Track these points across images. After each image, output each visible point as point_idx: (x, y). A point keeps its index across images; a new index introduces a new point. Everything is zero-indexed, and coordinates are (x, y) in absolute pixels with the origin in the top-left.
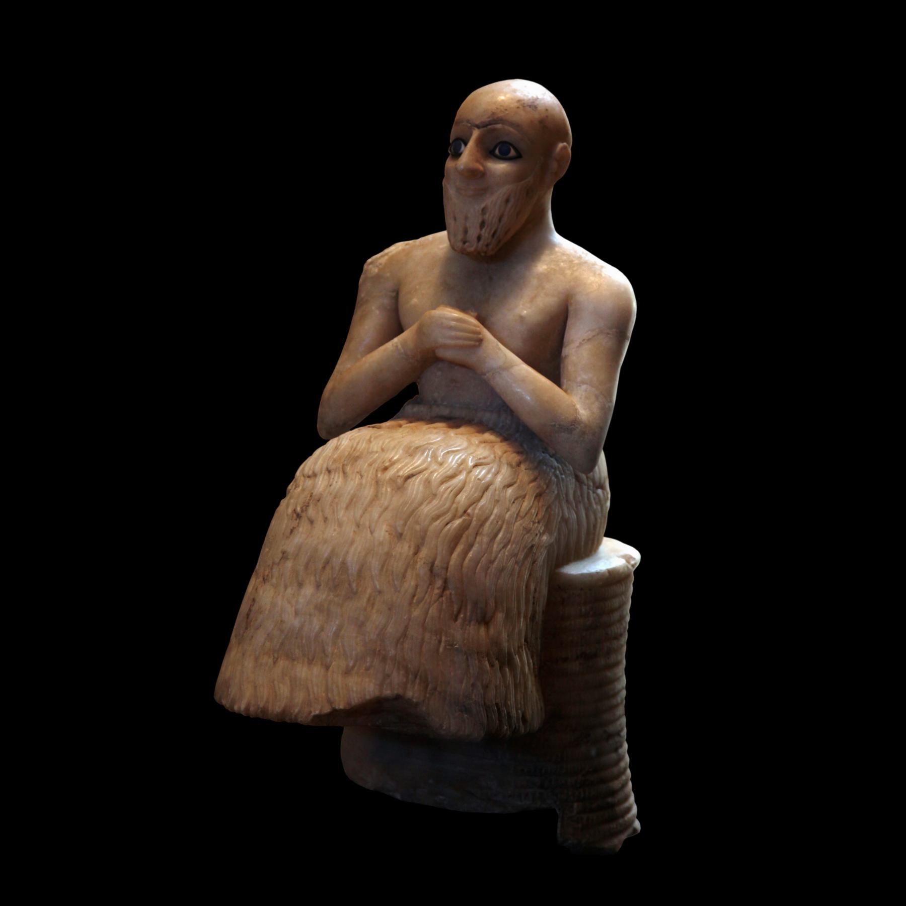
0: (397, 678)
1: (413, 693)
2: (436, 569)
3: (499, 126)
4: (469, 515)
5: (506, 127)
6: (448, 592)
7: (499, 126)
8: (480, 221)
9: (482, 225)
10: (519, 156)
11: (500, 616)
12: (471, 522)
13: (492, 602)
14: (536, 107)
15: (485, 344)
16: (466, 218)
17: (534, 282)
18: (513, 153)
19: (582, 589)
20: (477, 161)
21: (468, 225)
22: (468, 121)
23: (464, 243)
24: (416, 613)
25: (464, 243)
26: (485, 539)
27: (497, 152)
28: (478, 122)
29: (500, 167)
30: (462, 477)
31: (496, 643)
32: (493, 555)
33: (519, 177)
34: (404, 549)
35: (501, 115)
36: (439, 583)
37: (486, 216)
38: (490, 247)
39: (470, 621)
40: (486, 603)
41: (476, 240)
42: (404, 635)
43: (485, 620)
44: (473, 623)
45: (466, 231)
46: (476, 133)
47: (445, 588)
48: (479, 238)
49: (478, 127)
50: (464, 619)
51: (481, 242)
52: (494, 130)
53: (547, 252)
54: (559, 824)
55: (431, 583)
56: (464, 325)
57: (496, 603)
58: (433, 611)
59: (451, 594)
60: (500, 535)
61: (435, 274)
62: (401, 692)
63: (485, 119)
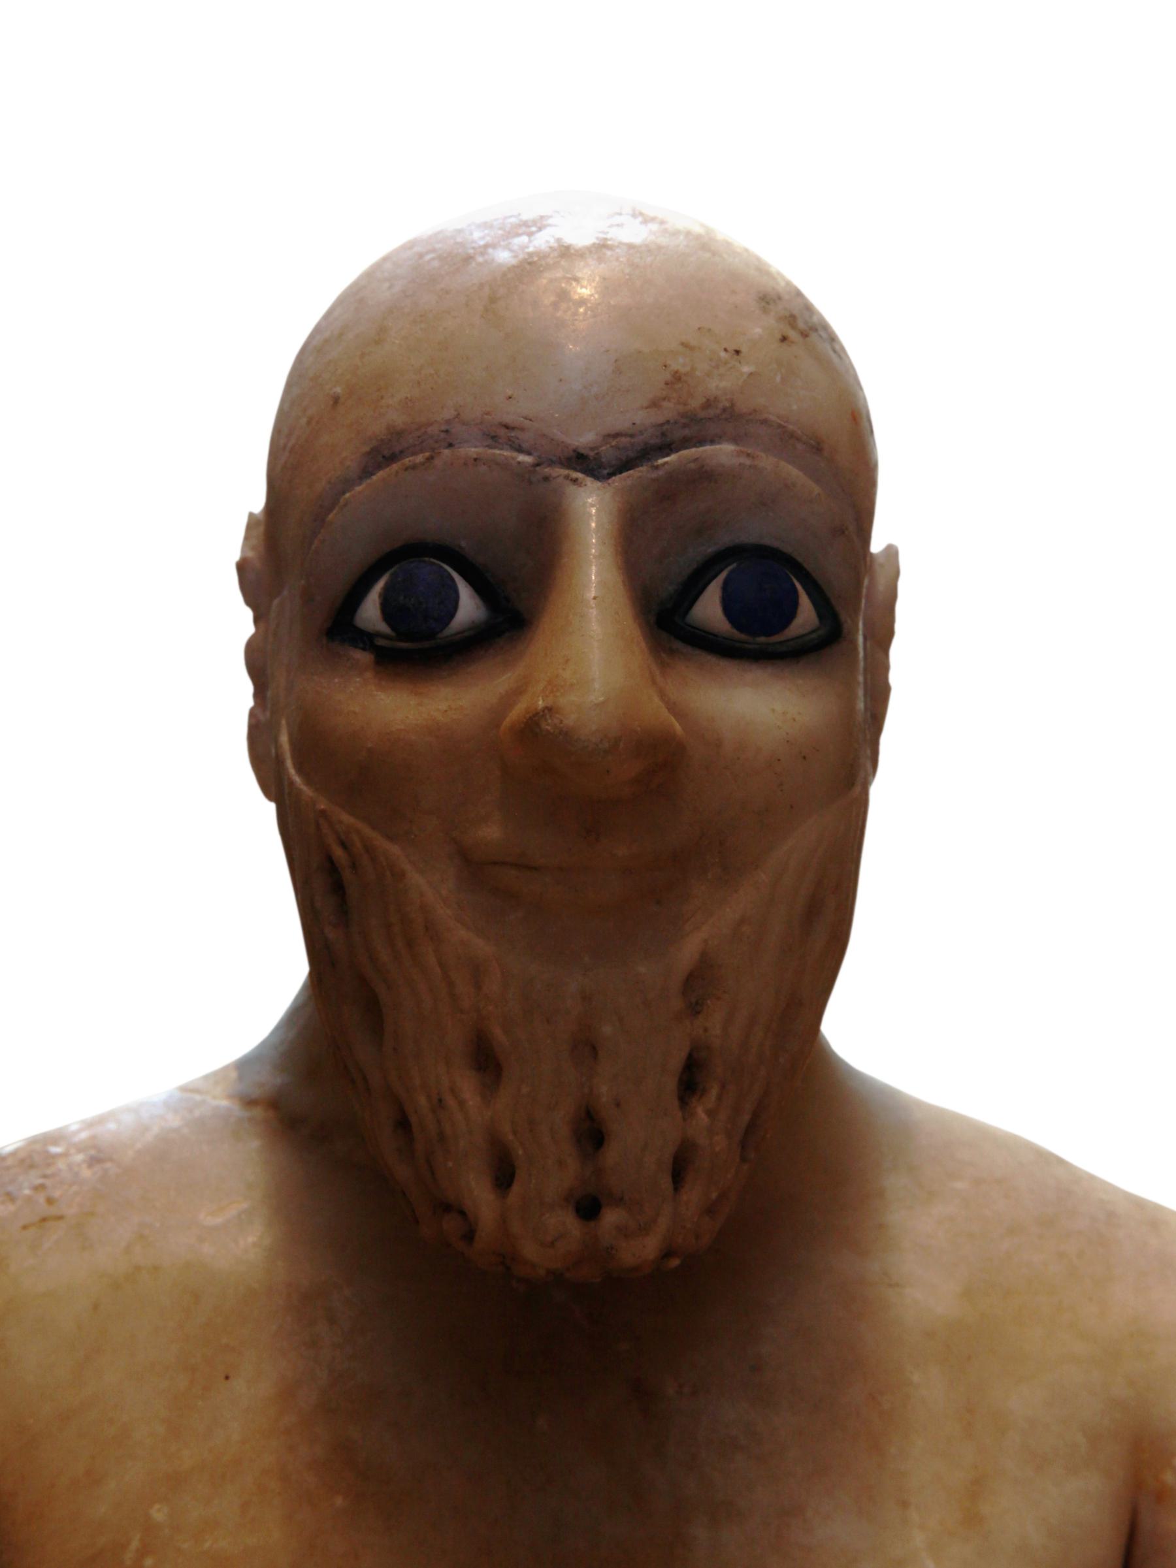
3: (723, 453)
5: (767, 462)
7: (722, 453)
8: (677, 1061)
9: (691, 1081)
16: (587, 1048)
17: (929, 1388)
21: (604, 1091)
22: (502, 434)
23: (588, 1208)
25: (588, 1208)
27: (709, 610)
28: (584, 439)
35: (719, 385)
37: (713, 1023)
41: (666, 1182)
45: (591, 1133)
46: (592, 510)
48: (680, 1168)
49: (586, 463)
51: (694, 1195)
52: (703, 476)
53: (895, 1183)
61: (248, 1404)
63: (632, 415)
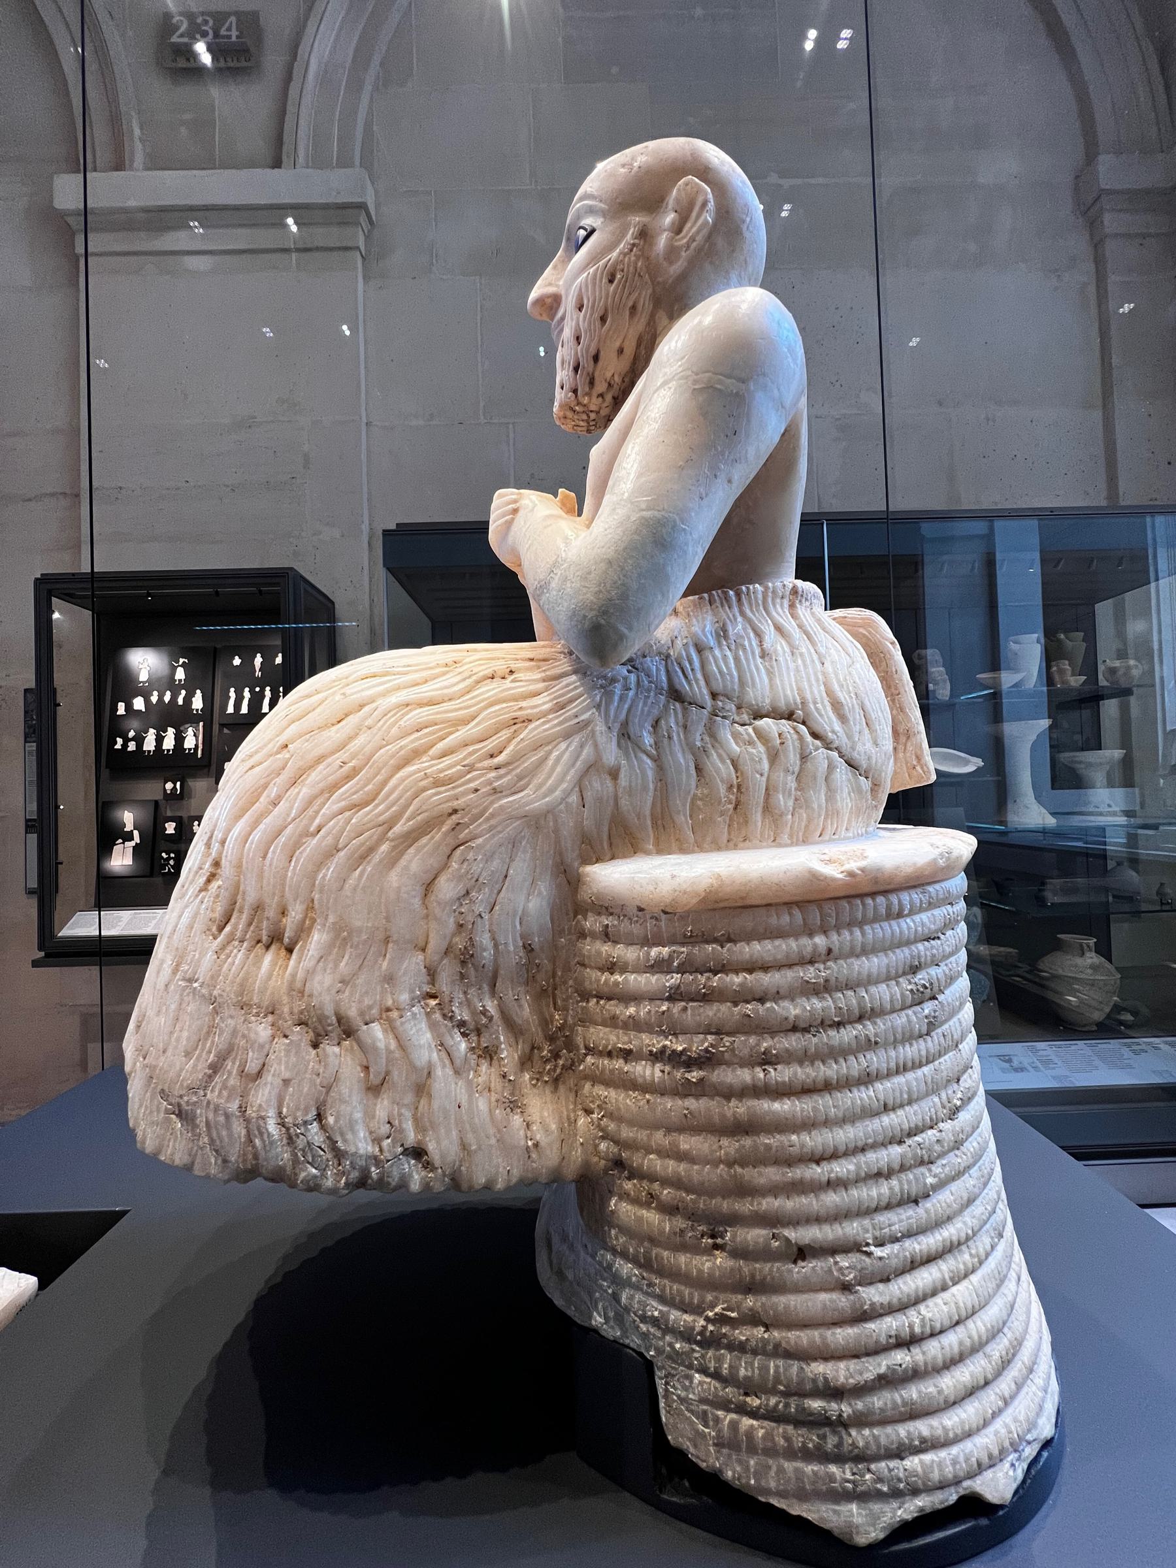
11: (317, 939)
13: (295, 913)
31: (299, 991)
43: (280, 941)
50: (230, 939)
54: (662, 1405)
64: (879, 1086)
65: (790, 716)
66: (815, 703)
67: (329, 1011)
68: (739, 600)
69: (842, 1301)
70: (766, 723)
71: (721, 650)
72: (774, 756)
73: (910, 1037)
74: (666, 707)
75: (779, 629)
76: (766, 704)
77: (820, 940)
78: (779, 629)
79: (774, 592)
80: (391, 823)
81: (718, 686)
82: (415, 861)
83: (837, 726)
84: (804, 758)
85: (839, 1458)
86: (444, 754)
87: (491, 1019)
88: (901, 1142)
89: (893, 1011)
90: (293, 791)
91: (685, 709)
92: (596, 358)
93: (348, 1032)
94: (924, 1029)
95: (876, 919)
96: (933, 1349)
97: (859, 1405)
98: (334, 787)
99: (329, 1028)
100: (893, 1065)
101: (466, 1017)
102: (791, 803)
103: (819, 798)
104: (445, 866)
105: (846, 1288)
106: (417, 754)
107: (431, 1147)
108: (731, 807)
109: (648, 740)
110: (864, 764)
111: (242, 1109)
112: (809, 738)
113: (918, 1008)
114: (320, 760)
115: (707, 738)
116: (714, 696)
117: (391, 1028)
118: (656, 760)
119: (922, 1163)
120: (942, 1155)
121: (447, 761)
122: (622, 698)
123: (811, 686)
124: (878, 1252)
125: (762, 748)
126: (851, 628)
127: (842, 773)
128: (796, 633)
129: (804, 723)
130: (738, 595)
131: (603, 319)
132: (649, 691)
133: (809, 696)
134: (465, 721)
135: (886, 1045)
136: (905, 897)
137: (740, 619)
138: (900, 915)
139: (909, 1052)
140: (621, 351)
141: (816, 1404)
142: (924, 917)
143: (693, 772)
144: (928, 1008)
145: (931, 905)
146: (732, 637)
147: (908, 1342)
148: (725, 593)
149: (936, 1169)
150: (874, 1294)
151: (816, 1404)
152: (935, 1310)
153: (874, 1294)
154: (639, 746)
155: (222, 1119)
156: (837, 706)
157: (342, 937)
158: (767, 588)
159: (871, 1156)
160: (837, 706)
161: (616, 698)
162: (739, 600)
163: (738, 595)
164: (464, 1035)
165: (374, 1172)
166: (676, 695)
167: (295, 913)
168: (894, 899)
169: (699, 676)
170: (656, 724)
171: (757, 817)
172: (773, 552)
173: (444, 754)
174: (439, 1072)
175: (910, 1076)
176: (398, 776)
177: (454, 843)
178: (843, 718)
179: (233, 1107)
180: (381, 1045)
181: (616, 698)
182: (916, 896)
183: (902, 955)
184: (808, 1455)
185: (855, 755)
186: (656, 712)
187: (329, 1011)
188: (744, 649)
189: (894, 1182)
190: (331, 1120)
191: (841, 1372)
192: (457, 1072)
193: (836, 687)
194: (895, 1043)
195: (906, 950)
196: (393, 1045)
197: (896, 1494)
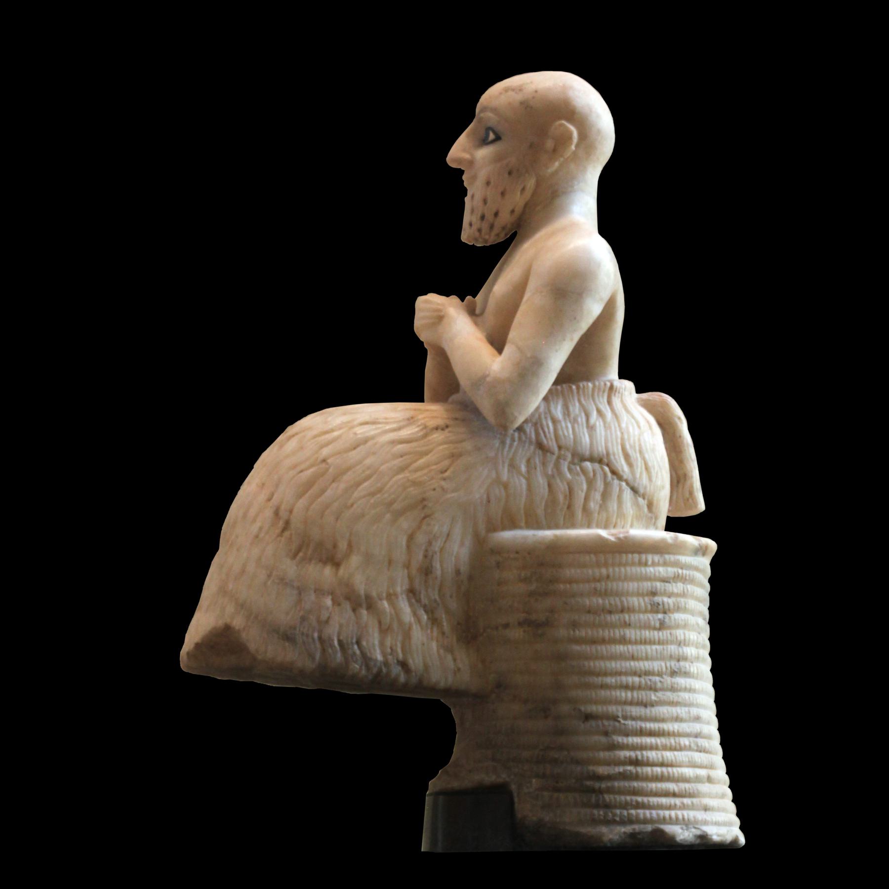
0: (230, 609)
1: (238, 623)
2: (281, 513)
4: (327, 464)
6: (287, 534)
10: (498, 138)
11: (355, 560)
12: (327, 470)
14: (521, 90)
15: (445, 320)
18: (492, 136)
19: (517, 553)
20: (464, 150)
24: (256, 552)
26: (342, 486)
29: (483, 153)
30: (336, 434)
32: (351, 501)
33: (498, 158)
34: (262, 497)
36: (281, 524)
38: (483, 231)
39: (310, 560)
40: (335, 546)
42: (243, 571)
44: (313, 562)
47: (284, 530)
48: (471, 225)
50: (303, 559)
55: (273, 525)
56: (428, 306)
57: (350, 545)
58: (270, 550)
59: (291, 535)
60: (366, 484)
62: (228, 621)
64: (630, 647)
65: (600, 461)
66: (614, 455)
67: (362, 593)
68: (578, 392)
69: (603, 739)
70: (588, 465)
71: (566, 423)
72: (591, 483)
73: (647, 626)
74: (534, 453)
75: (599, 412)
76: (587, 453)
77: (604, 571)
78: (599, 412)
79: (599, 389)
80: (391, 503)
81: (563, 442)
82: (405, 524)
83: (626, 468)
84: (607, 485)
85: (597, 806)
86: (417, 470)
87: (438, 604)
88: (640, 676)
89: (640, 611)
90: (334, 485)
91: (544, 456)
92: (496, 214)
93: (371, 605)
94: (658, 625)
95: (633, 564)
96: (648, 770)
97: (609, 784)
98: (358, 484)
99: (359, 602)
100: (638, 638)
101: (427, 602)
102: (597, 508)
103: (613, 505)
104: (419, 527)
105: (606, 734)
106: (402, 469)
107: (410, 661)
108: (566, 507)
109: (523, 469)
110: (642, 491)
111: (320, 638)
112: (609, 474)
113: (654, 615)
114: (349, 469)
115: (555, 470)
116: (560, 448)
117: (392, 604)
118: (528, 479)
119: (651, 689)
120: (662, 689)
121: (419, 474)
122: (511, 446)
123: (613, 445)
124: (622, 722)
125: (583, 478)
126: (650, 407)
127: (628, 494)
128: (609, 415)
129: (608, 465)
130: (578, 388)
131: (503, 194)
132: (525, 442)
133: (611, 452)
134: (426, 453)
135: (635, 627)
136: (650, 558)
137: (577, 404)
138: (646, 565)
139: (647, 634)
140: (513, 211)
141: (589, 783)
142: (661, 569)
143: (546, 487)
144: (660, 616)
145: (665, 564)
146: (572, 416)
147: (636, 763)
148: (571, 387)
149: (660, 694)
150: (620, 739)
151: (589, 783)
152: (652, 755)
153: (620, 739)
154: (519, 472)
155: (311, 640)
156: (627, 456)
157: (368, 558)
158: (594, 386)
159: (624, 679)
160: (627, 456)
161: (507, 446)
162: (578, 392)
163: (578, 388)
164: (426, 612)
165: (384, 670)
166: (540, 446)
167: (343, 546)
168: (643, 557)
169: (553, 437)
170: (528, 461)
171: (579, 514)
172: (603, 360)
173: (417, 470)
174: (414, 627)
175: (648, 647)
176: (395, 479)
177: (423, 515)
178: (630, 465)
179: (316, 635)
180: (388, 610)
181: (507, 446)
182: (657, 558)
183: (647, 585)
184: (585, 805)
185: (636, 485)
186: (528, 454)
187: (362, 593)
188: (578, 424)
189: (635, 694)
190: (364, 643)
191: (602, 770)
192: (422, 628)
193: (628, 447)
194: (640, 628)
195: (649, 584)
196: (393, 612)
197: (623, 822)
